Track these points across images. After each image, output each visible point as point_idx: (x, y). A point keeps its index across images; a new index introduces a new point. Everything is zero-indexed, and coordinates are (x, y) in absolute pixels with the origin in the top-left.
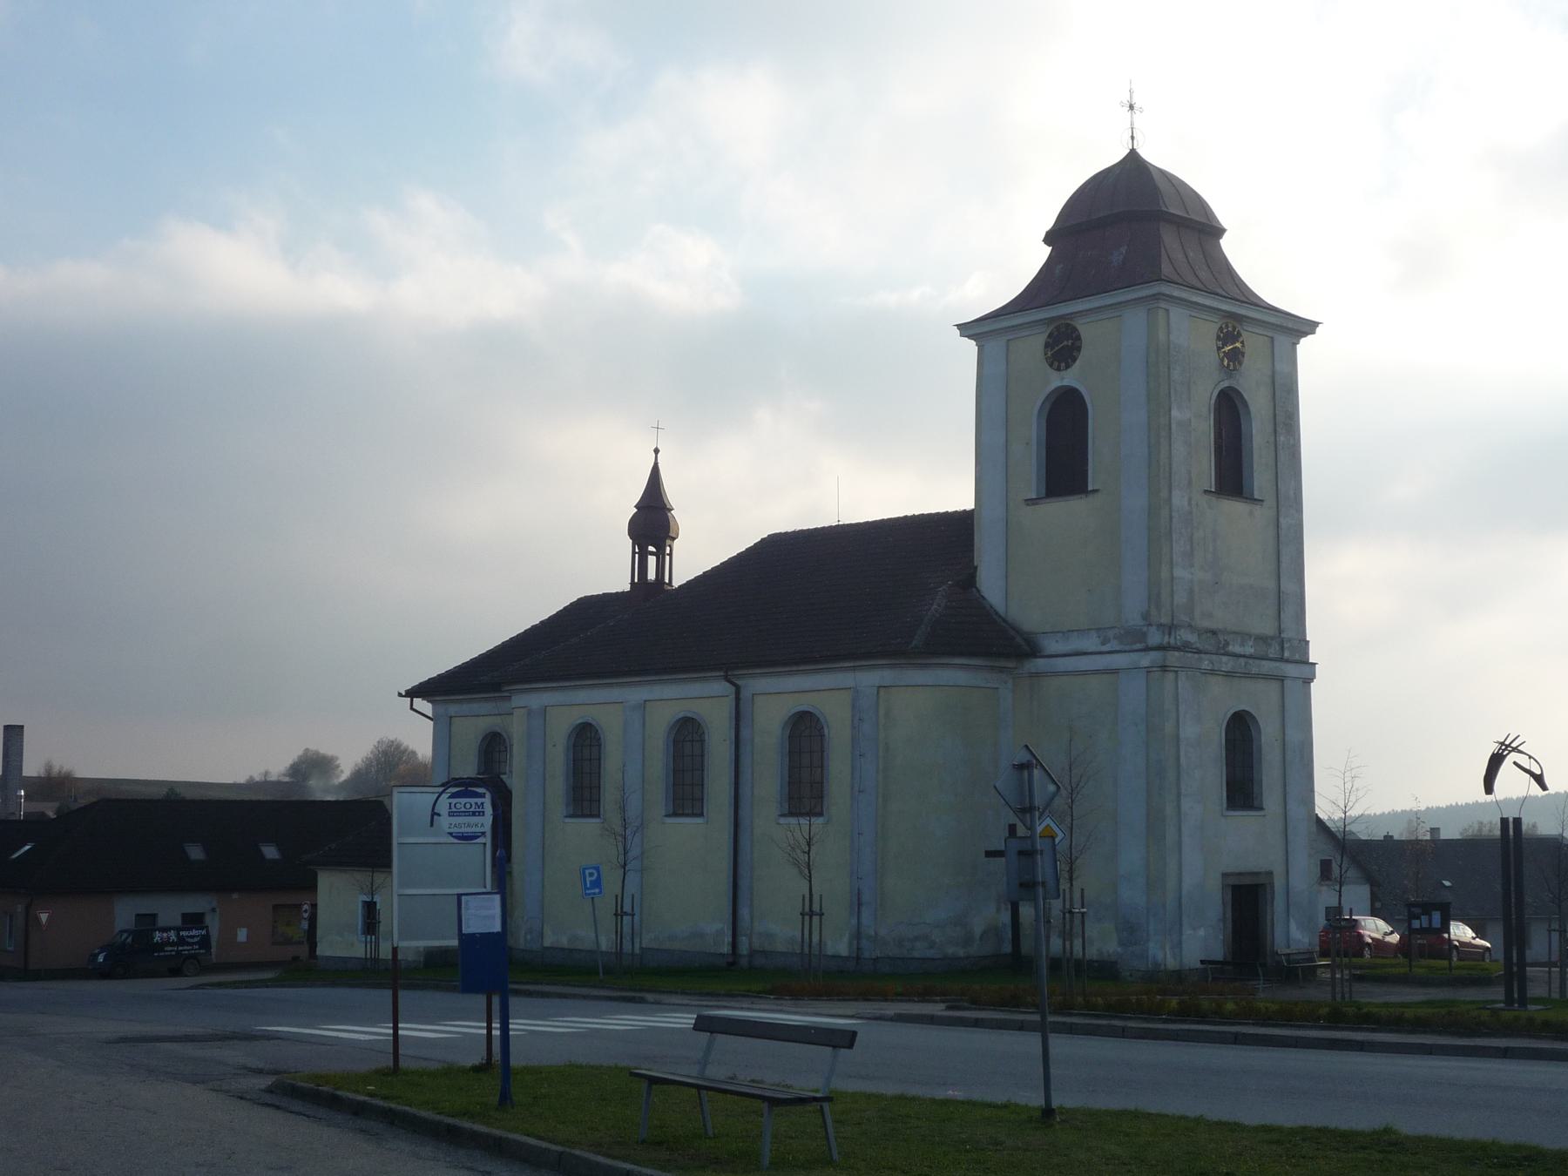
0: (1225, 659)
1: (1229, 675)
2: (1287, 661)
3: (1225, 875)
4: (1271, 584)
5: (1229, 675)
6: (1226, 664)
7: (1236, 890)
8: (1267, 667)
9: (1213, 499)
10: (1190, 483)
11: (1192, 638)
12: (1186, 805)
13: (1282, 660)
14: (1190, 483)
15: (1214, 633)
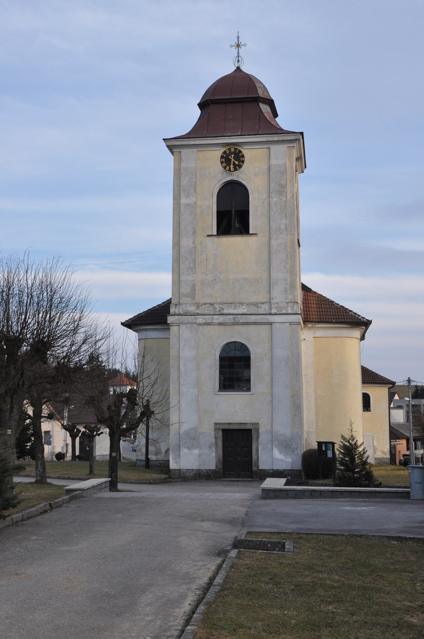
0: (215, 317)
1: (220, 324)
2: (276, 314)
3: (215, 424)
4: (265, 276)
5: (220, 324)
6: (221, 319)
7: (224, 430)
8: (253, 318)
9: (216, 239)
10: (194, 232)
11: (192, 309)
12: (183, 389)
13: (271, 314)
14: (194, 232)
15: (211, 304)
